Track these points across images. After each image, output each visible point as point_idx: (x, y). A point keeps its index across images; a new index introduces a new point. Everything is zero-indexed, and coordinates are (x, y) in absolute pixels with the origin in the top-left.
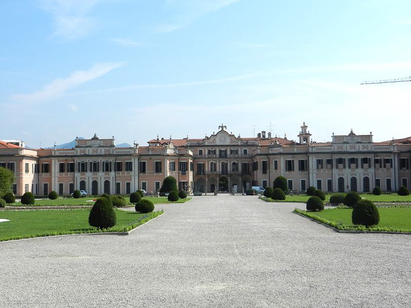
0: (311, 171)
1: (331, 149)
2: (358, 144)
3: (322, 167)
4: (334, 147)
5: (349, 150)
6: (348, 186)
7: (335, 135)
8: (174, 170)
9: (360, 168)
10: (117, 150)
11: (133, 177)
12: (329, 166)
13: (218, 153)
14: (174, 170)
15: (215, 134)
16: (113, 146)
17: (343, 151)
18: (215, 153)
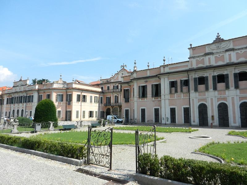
0: (162, 97)
1: (187, 66)
2: (228, 53)
3: (176, 91)
4: (191, 62)
5: (213, 63)
6: (213, 117)
7: (192, 46)
8: (62, 101)
10: (28, 87)
12: (185, 88)
14: (62, 101)
16: (26, 85)
17: (205, 66)
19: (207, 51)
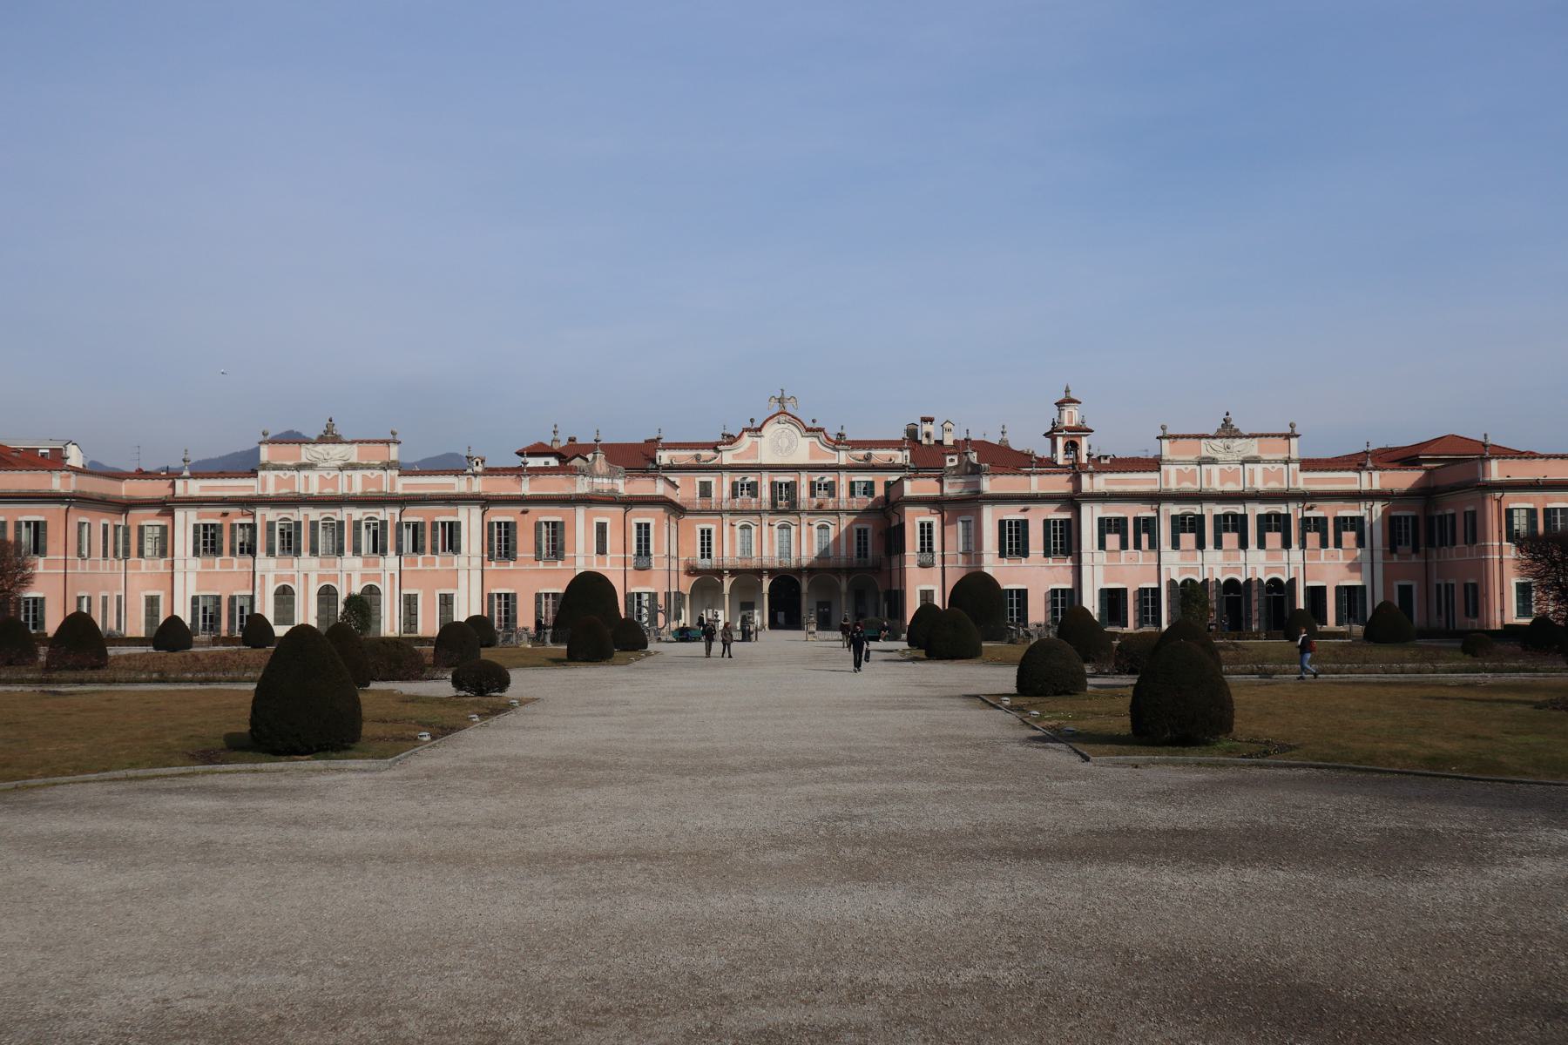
0: (1085, 558)
4: (1167, 472)
9: (391, 553)
11: (463, 575)
13: (765, 493)
15: (757, 424)
18: (755, 495)
19: (1204, 453)
